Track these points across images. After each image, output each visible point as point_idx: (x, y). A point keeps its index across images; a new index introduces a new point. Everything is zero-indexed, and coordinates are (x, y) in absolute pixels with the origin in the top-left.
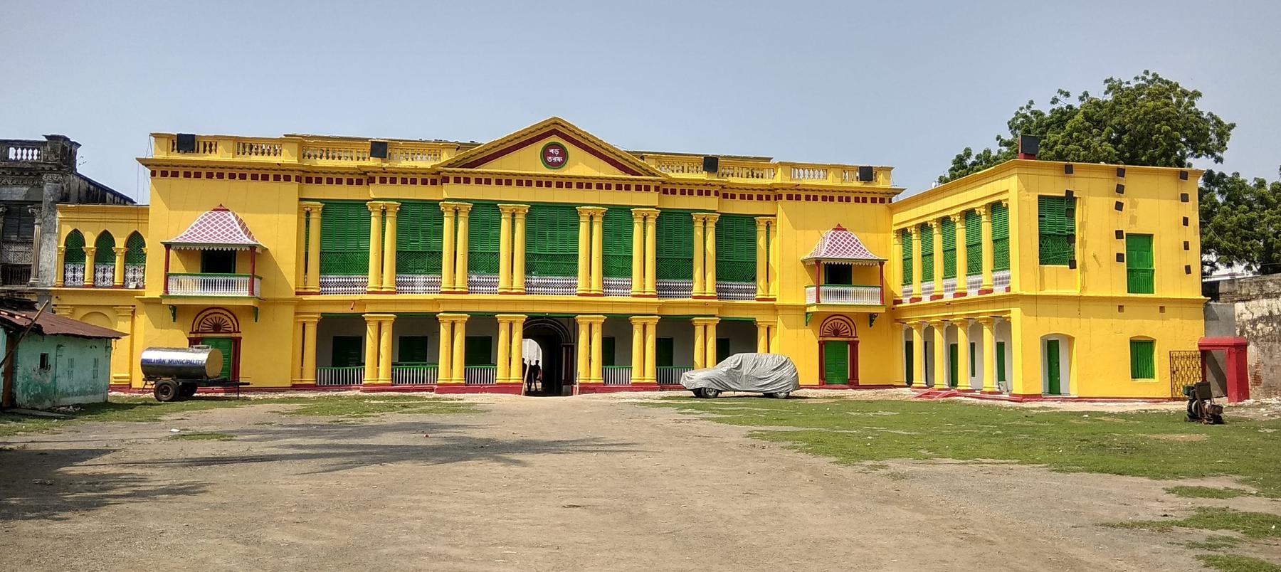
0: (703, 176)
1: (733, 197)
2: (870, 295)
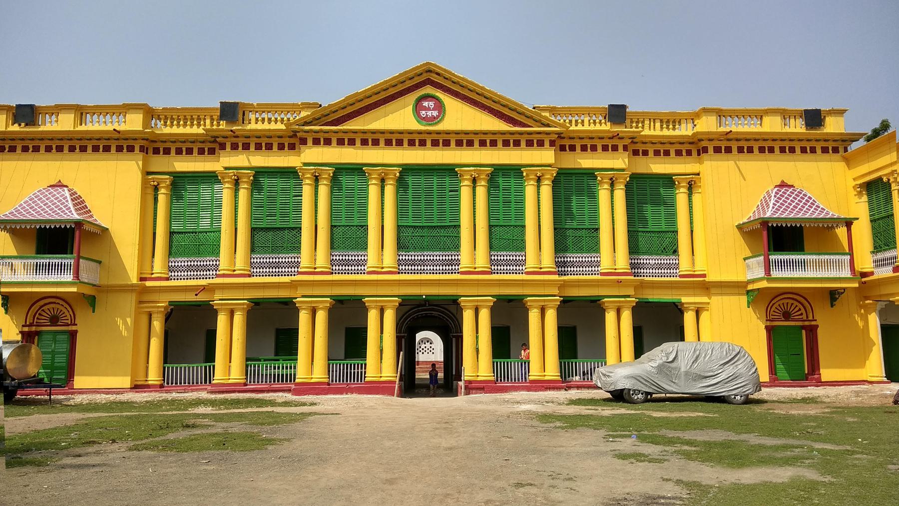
0: (607, 127)
1: (645, 153)
2: (839, 264)
